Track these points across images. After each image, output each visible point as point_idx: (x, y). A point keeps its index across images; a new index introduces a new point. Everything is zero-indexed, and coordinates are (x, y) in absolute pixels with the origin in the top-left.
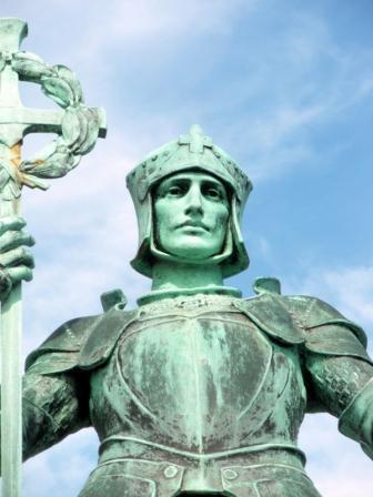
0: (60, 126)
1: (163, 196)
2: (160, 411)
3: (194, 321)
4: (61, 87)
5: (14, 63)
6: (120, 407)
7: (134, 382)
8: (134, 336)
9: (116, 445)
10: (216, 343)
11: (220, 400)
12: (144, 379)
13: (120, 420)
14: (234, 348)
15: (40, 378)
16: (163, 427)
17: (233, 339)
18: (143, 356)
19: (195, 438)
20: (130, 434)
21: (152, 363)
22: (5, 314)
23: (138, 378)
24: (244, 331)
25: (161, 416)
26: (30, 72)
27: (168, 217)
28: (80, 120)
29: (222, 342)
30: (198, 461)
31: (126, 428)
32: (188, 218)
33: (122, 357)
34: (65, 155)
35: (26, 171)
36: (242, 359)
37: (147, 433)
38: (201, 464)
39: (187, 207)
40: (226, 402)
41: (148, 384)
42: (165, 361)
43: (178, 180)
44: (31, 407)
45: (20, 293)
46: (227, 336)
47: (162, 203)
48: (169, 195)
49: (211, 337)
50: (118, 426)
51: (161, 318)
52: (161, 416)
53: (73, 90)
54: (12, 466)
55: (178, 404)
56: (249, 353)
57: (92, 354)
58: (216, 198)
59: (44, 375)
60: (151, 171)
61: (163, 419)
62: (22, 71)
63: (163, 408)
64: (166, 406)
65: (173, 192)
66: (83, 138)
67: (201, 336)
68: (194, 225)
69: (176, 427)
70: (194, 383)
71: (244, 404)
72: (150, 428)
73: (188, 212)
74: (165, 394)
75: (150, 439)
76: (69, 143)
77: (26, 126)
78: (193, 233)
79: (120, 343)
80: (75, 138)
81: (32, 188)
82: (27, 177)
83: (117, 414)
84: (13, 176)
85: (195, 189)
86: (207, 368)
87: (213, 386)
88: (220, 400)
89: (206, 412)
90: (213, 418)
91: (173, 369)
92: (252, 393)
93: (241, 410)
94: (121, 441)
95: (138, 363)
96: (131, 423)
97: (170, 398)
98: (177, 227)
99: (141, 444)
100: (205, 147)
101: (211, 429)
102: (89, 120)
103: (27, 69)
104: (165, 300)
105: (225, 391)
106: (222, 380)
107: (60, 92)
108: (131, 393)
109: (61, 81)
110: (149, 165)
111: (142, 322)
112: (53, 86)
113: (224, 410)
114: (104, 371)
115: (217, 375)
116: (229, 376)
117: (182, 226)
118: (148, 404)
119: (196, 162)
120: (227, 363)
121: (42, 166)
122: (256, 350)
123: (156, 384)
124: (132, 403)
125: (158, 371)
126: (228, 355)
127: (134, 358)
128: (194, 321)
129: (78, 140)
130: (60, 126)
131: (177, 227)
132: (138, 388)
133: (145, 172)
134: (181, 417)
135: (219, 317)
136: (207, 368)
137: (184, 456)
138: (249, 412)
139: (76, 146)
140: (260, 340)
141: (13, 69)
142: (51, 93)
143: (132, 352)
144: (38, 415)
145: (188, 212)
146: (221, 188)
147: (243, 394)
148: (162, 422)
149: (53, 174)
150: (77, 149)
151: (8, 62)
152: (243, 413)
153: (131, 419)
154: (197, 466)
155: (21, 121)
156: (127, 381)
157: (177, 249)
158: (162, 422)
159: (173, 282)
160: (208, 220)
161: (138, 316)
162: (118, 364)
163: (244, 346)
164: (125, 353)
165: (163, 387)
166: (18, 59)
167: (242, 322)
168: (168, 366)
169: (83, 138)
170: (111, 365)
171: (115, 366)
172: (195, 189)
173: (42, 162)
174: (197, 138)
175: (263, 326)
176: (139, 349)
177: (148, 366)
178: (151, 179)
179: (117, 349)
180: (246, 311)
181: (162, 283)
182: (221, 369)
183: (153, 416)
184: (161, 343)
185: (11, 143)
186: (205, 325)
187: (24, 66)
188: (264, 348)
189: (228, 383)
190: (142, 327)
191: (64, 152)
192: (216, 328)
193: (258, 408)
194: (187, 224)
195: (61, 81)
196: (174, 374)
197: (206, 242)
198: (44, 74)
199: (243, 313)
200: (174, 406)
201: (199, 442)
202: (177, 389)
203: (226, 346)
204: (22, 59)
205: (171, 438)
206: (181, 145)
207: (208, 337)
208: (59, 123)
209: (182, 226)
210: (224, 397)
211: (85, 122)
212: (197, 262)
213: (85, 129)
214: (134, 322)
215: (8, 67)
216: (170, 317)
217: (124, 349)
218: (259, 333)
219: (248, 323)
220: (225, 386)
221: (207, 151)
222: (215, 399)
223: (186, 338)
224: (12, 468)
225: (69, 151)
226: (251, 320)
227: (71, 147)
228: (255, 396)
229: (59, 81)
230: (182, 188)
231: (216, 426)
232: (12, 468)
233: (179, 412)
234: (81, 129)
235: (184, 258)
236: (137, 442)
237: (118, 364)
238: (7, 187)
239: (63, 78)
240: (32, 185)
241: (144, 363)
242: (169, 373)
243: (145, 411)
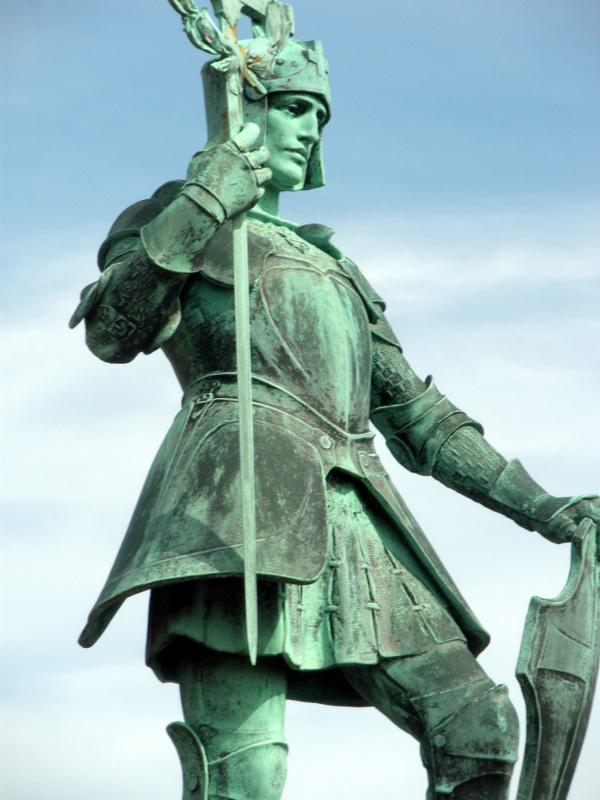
1: (278, 108)
2: (314, 373)
16: (315, 390)
18: (293, 303)
19: (343, 414)
20: (277, 382)
21: (305, 316)
23: (290, 326)
25: (314, 378)
27: (281, 135)
30: (346, 438)
32: (300, 145)
33: (269, 293)
37: (298, 389)
38: (348, 443)
39: (304, 133)
42: (318, 320)
48: (287, 111)
55: (331, 372)
63: (317, 371)
65: (292, 110)
69: (328, 396)
72: (302, 385)
73: (302, 139)
74: (318, 356)
75: (301, 396)
89: (351, 390)
91: (325, 333)
94: (269, 387)
95: (288, 308)
97: (323, 363)
98: (287, 149)
99: (295, 400)
104: (256, 221)
105: (361, 369)
117: (292, 150)
119: (323, 88)
121: (259, 63)
124: (282, 350)
125: (311, 327)
127: (284, 301)
131: (287, 149)
132: (290, 337)
134: (333, 387)
136: (350, 341)
137: (334, 429)
143: (280, 292)
145: (302, 139)
148: (314, 385)
153: (279, 367)
154: (344, 444)
156: (276, 323)
158: (314, 385)
162: (264, 299)
164: (273, 290)
165: (316, 348)
176: (288, 294)
177: (301, 318)
178: (277, 84)
183: (307, 376)
194: (298, 151)
196: (326, 337)
200: (327, 372)
201: (346, 419)
202: (330, 355)
205: (322, 405)
208: (263, 13)
209: (292, 150)
214: (271, 255)
230: (300, 109)
233: (331, 381)
236: (291, 397)
241: (295, 312)
242: (321, 335)
243: (298, 365)
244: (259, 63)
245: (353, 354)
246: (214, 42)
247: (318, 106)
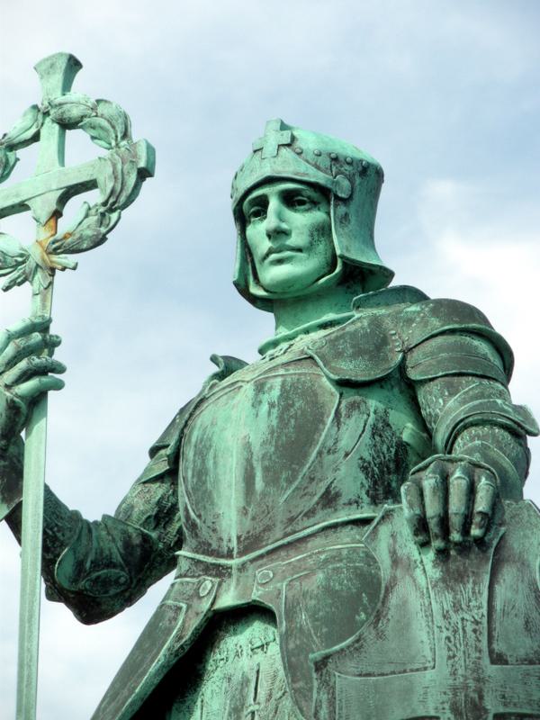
5: (52, 112)
11: (259, 484)
19: (230, 540)
26: (70, 118)
29: (272, 405)
30: (231, 568)
36: (293, 421)
38: (234, 572)
40: (267, 484)
42: (210, 446)
44: (124, 527)
53: (113, 127)
58: (306, 206)
66: (118, 188)
68: (279, 251)
69: (214, 530)
71: (290, 481)
77: (61, 191)
78: (280, 262)
80: (108, 191)
84: (40, 264)
85: (274, 204)
87: (252, 468)
89: (242, 503)
101: (248, 523)
105: (266, 470)
113: (264, 495)
116: (273, 449)
119: (267, 171)
121: (69, 240)
126: (275, 422)
134: (218, 516)
136: (248, 446)
137: (219, 565)
139: (111, 201)
141: (53, 121)
146: (309, 192)
150: (114, 203)
151: (46, 114)
152: (289, 492)
154: (230, 575)
155: (54, 187)
173: (70, 234)
182: (264, 443)
196: (215, 463)
198: (85, 116)
201: (234, 544)
210: (265, 477)
211: (119, 167)
220: (267, 463)
222: (254, 484)
234: (116, 178)
235: (284, 293)
244: (69, 240)
245: (249, 461)
246: (5, 262)
247: (272, 192)
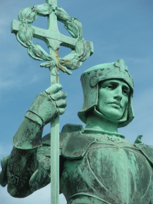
0: (75, 46)
1: (104, 87)
2: (110, 188)
3: (122, 149)
4: (75, 28)
5: (56, 11)
6: (88, 180)
7: (97, 171)
8: (95, 149)
9: (86, 198)
10: (133, 162)
11: (136, 189)
12: (102, 171)
13: (88, 186)
14: (140, 166)
15: (45, 158)
16: (111, 195)
17: (139, 162)
18: (101, 160)
20: (93, 194)
21: (106, 165)
22: (52, 128)
23: (99, 170)
24: (142, 159)
25: (110, 190)
26: (62, 17)
27: (106, 98)
28: (84, 46)
29: (135, 162)
31: (91, 191)
32: (115, 100)
33: (90, 158)
34: (77, 61)
35: (62, 64)
36: (143, 172)
37: (103, 196)
39: (116, 95)
40: (138, 190)
41: (104, 174)
43: (113, 82)
44: (43, 170)
45: (59, 120)
46: (137, 159)
47: (103, 90)
48: (107, 88)
49: (130, 159)
50: (86, 189)
51: (107, 144)
52: (110, 190)
53: (80, 31)
54: (56, 199)
55: (118, 186)
56: (145, 170)
57: (74, 152)
58: (126, 94)
59: (47, 156)
60: (100, 75)
61: (111, 191)
62: (59, 16)
63: (111, 186)
64: (113, 186)
65: (110, 87)
66: (84, 55)
67: (126, 157)
68: (117, 104)
69: (117, 197)
70: (126, 178)
71: (144, 193)
72: (104, 194)
73: (115, 98)
74: (112, 180)
75: (104, 199)
76: (79, 55)
77: (62, 42)
78: (116, 108)
79: (89, 151)
80: (82, 54)
81: (64, 72)
82: (63, 66)
83: (86, 184)
84: (57, 65)
85: (120, 88)
86: (131, 173)
87: (133, 182)
88: (136, 189)
89: (130, 193)
90: (133, 196)
91: (116, 170)
92: (146, 189)
93: (143, 195)
94: (89, 197)
95: (99, 163)
96: (94, 190)
97: (115, 183)
98: (109, 103)
99: (100, 200)
100: (126, 70)
101: (132, 201)
102: (87, 47)
103: (61, 15)
104: (99, 134)
105: (137, 185)
106: (137, 180)
107: (74, 30)
108: (95, 176)
109: (75, 25)
110: (99, 72)
111: (98, 144)
112: (71, 26)
113: (137, 194)
114: (79, 162)
115: (134, 178)
116: (139, 179)
117: (112, 103)
118: (104, 183)
119: (122, 76)
120: (138, 173)
121: (68, 63)
122: (147, 169)
123: (108, 172)
124: (95, 180)
125: (109, 169)
126: (138, 169)
127: (97, 160)
128: (122, 149)
129: (82, 55)
130: (75, 46)
131: (109, 103)
132: (99, 174)
133: (96, 74)
134: (120, 193)
135: (132, 150)
136: (131, 173)
138: (145, 197)
139: (81, 57)
140: (148, 164)
141: (55, 14)
142: (69, 29)
143: (95, 157)
144: (45, 174)
145: (115, 98)
146: (129, 90)
147: (143, 188)
148: (110, 193)
149: (72, 68)
150: (82, 59)
151: (54, 10)
152: (143, 197)
153: (94, 188)
156: (93, 170)
157: (107, 113)
158: (110, 193)
159: (100, 126)
160: (122, 103)
161: (96, 141)
162: (88, 161)
163: (143, 166)
164: (92, 157)
165: (111, 177)
166: (58, 10)
167: (139, 154)
168: (114, 167)
169: (84, 55)
170: (84, 160)
171: (86, 161)
172: (120, 88)
173: (69, 61)
174: (122, 65)
175: (149, 159)
176: (99, 156)
177: (104, 166)
178: (100, 78)
179: (87, 154)
180: (141, 150)
181: (95, 126)
182: (136, 175)
183: (106, 189)
184: (109, 156)
185: (55, 49)
186: (127, 152)
187: (60, 14)
188: (149, 169)
189: (138, 182)
190: (98, 146)
191: (77, 59)
192: (131, 155)
193: (148, 195)
194: (114, 103)
195: (75, 25)
196: (117, 172)
197: (118, 112)
198: (68, 20)
199: (140, 151)
200: (117, 186)
202: (118, 179)
203: (137, 164)
204: (59, 10)
205: (114, 201)
206: (116, 67)
207: (130, 159)
208: (74, 45)
209: (112, 103)
210: (137, 187)
211: (86, 47)
212: (112, 120)
213: (86, 51)
214: (94, 143)
215: (53, 12)
216: (110, 145)
217: (90, 155)
218: (147, 161)
219: (142, 155)
220: (138, 183)
221: (126, 72)
222: (134, 188)
223: (120, 157)
224: (56, 201)
225: (79, 59)
226: (143, 155)
227: (79, 57)
228: (147, 190)
229: (75, 25)
230: (114, 86)
231: (134, 200)
232: (56, 201)
233: (119, 190)
234: (84, 50)
235: (108, 117)
236: (98, 199)
237: (88, 161)
238: (54, 69)
239: (76, 24)
240: (65, 71)
241: (101, 164)
242: (114, 171)
243: (102, 185)
244: (68, 63)
245: (132, 179)
246: (42, 56)
247: (121, 84)
